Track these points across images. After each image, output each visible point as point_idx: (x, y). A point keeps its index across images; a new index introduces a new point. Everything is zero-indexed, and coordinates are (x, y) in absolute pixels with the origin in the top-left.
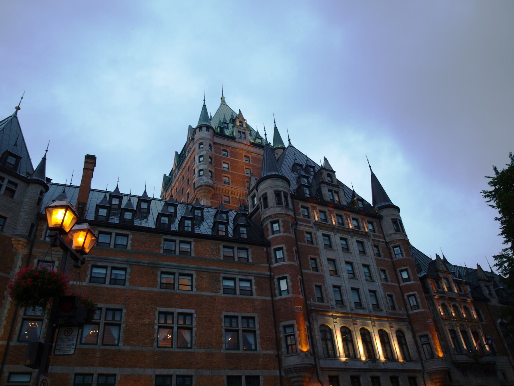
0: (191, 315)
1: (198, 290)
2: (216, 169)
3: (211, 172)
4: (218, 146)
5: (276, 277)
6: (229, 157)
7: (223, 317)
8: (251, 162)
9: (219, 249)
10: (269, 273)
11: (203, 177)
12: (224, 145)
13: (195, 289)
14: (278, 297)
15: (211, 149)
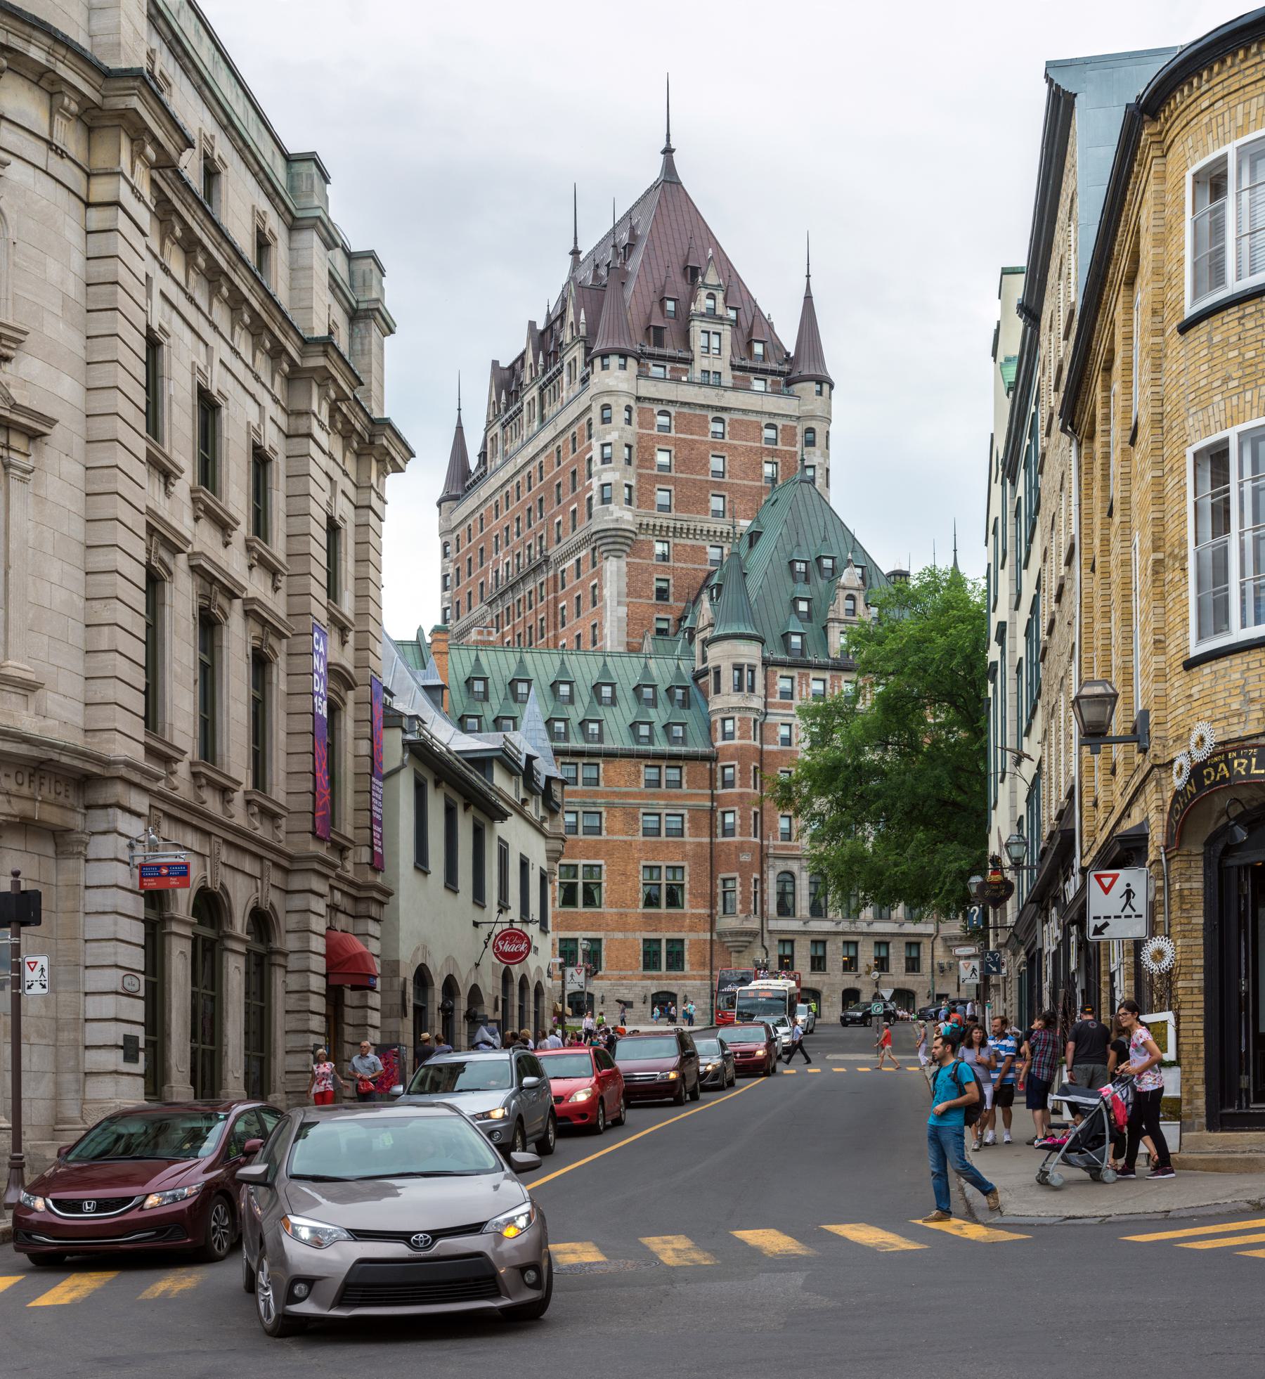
0: (600, 866)
1: (608, 833)
2: (640, 476)
3: (629, 487)
4: (647, 405)
5: (720, 810)
6: (673, 434)
7: (641, 868)
8: (727, 436)
9: (639, 771)
10: (709, 804)
11: (612, 507)
12: (661, 400)
13: (604, 832)
14: (720, 839)
15: (629, 422)
